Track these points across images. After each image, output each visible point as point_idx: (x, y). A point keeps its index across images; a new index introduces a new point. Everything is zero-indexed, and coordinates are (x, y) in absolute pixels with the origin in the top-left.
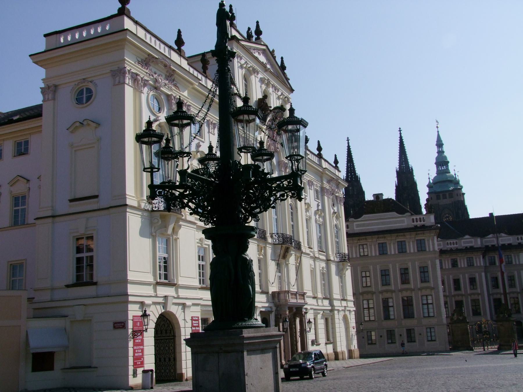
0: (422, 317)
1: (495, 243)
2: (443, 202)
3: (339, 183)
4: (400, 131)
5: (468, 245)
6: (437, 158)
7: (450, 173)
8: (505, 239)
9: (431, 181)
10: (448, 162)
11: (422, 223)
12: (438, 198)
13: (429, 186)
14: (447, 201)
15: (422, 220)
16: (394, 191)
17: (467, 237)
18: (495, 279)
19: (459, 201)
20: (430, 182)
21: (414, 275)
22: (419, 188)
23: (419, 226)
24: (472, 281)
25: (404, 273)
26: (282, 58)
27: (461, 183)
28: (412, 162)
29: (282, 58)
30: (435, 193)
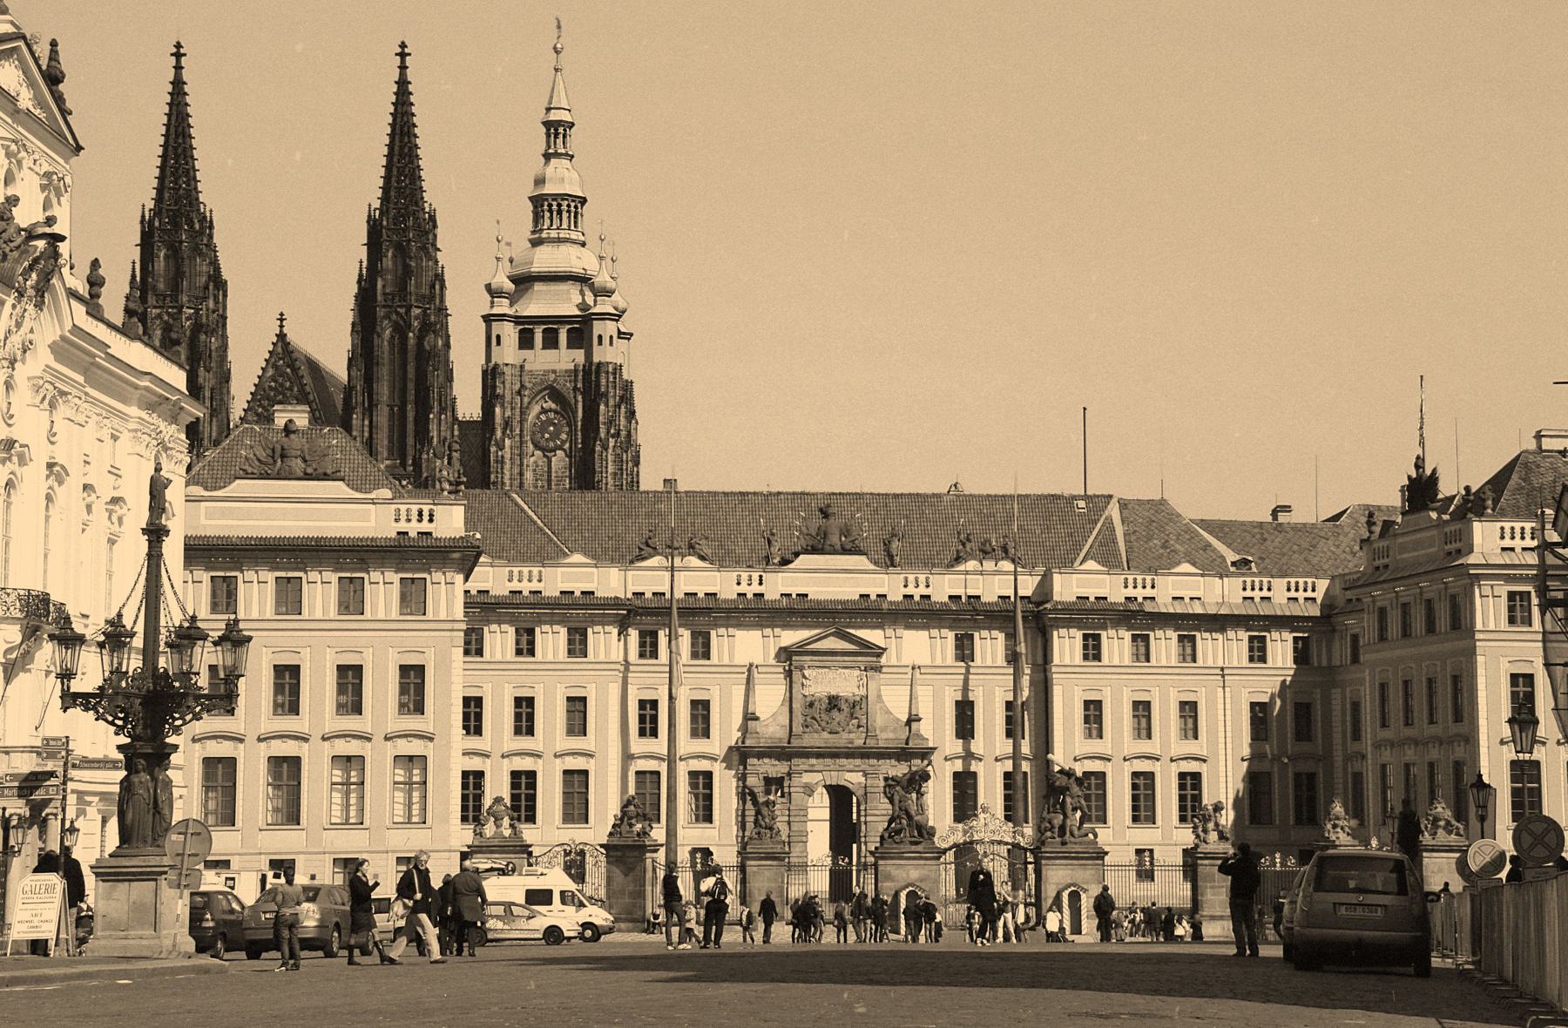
0: (388, 823)
1: (666, 588)
2: (542, 360)
3: (182, 408)
4: (403, 55)
5: (578, 587)
6: (540, 181)
8: (699, 579)
10: (584, 201)
11: (425, 526)
12: (526, 341)
13: (494, 292)
14: (565, 359)
15: (426, 517)
16: (350, 303)
17: (577, 558)
18: (648, 709)
19: (599, 364)
21: (381, 689)
22: (452, 300)
23: (413, 534)
24: (577, 706)
25: (350, 678)
26: (54, 44)
28: (437, 190)
29: (54, 44)
30: (518, 320)
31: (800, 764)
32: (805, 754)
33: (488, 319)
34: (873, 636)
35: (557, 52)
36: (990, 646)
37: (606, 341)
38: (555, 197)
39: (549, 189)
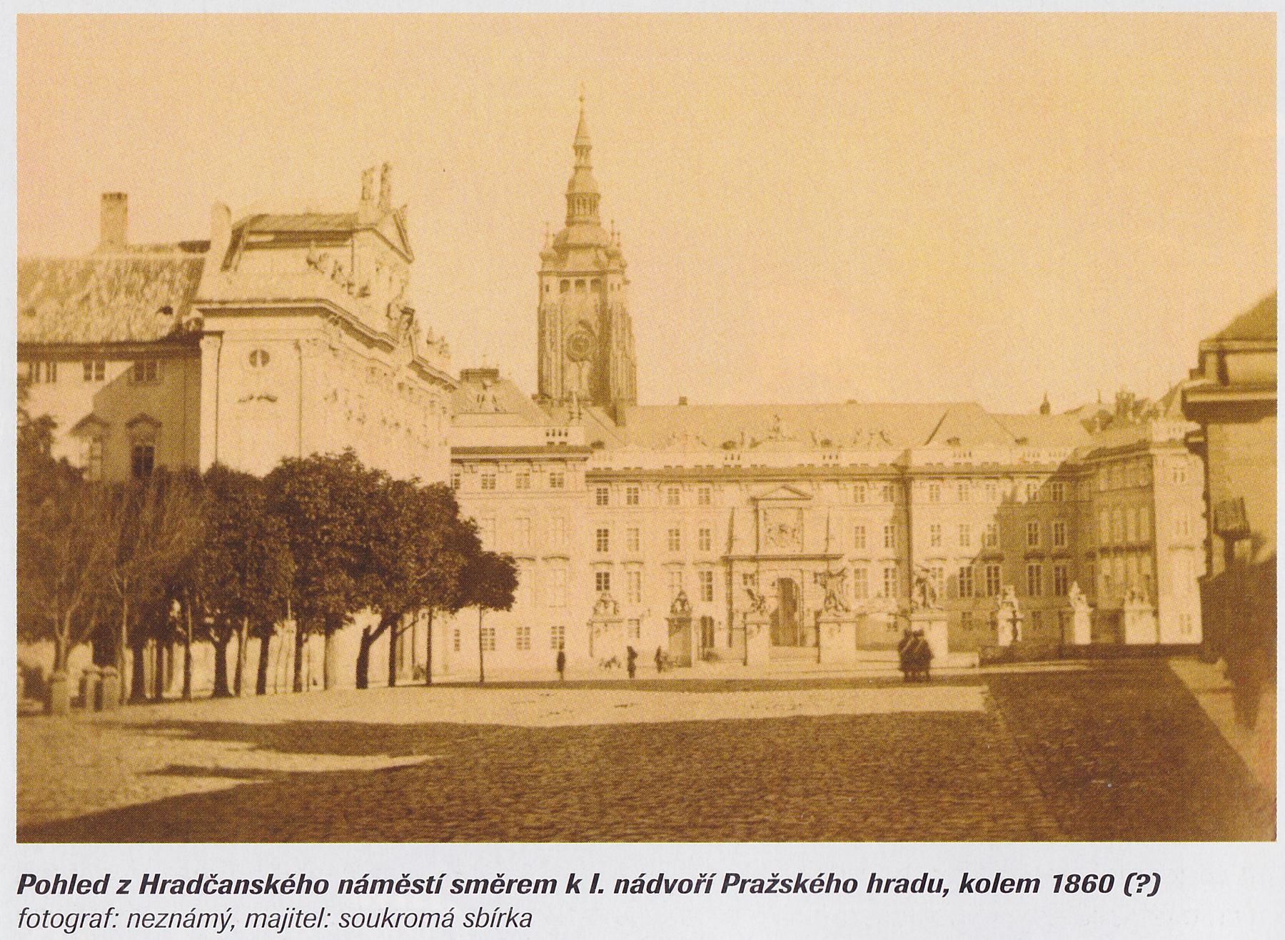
6: (572, 184)
7: (599, 224)
9: (551, 241)
13: (545, 258)
20: (546, 244)
27: (626, 256)
31: (764, 565)
32: (767, 559)
33: (541, 274)
34: (804, 487)
35: (581, 100)
36: (875, 491)
37: (615, 286)
38: (581, 195)
39: (577, 189)
